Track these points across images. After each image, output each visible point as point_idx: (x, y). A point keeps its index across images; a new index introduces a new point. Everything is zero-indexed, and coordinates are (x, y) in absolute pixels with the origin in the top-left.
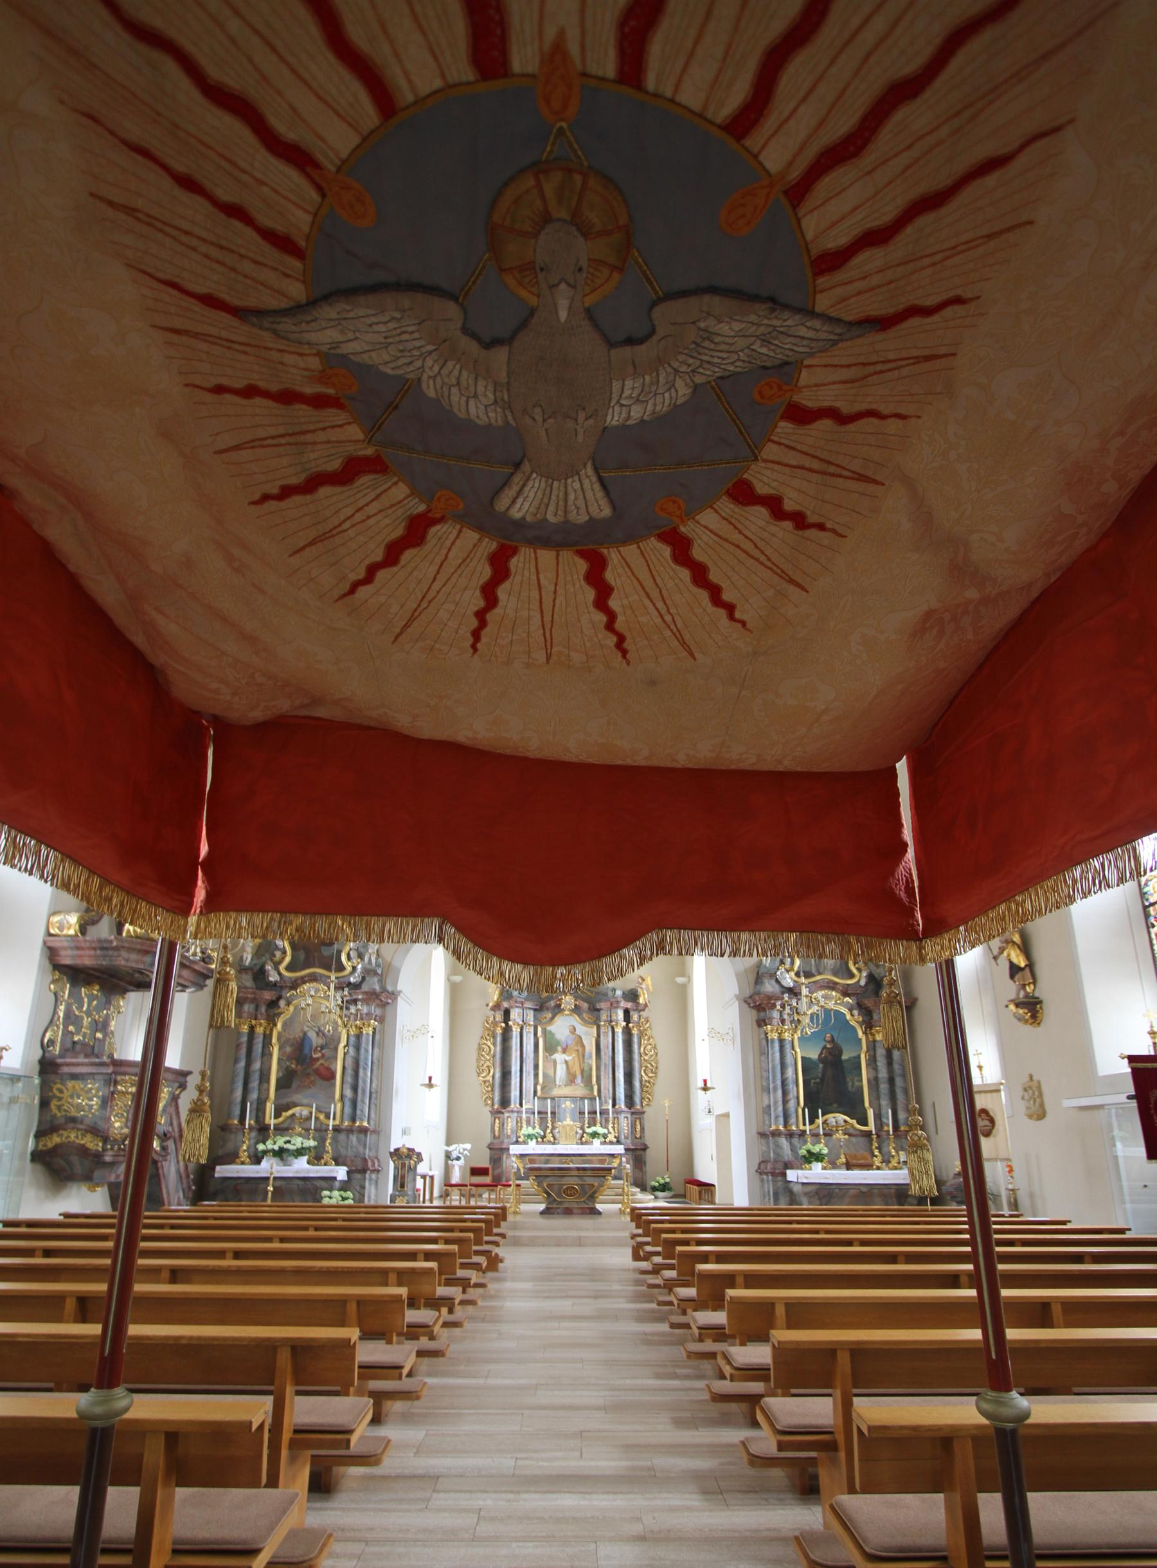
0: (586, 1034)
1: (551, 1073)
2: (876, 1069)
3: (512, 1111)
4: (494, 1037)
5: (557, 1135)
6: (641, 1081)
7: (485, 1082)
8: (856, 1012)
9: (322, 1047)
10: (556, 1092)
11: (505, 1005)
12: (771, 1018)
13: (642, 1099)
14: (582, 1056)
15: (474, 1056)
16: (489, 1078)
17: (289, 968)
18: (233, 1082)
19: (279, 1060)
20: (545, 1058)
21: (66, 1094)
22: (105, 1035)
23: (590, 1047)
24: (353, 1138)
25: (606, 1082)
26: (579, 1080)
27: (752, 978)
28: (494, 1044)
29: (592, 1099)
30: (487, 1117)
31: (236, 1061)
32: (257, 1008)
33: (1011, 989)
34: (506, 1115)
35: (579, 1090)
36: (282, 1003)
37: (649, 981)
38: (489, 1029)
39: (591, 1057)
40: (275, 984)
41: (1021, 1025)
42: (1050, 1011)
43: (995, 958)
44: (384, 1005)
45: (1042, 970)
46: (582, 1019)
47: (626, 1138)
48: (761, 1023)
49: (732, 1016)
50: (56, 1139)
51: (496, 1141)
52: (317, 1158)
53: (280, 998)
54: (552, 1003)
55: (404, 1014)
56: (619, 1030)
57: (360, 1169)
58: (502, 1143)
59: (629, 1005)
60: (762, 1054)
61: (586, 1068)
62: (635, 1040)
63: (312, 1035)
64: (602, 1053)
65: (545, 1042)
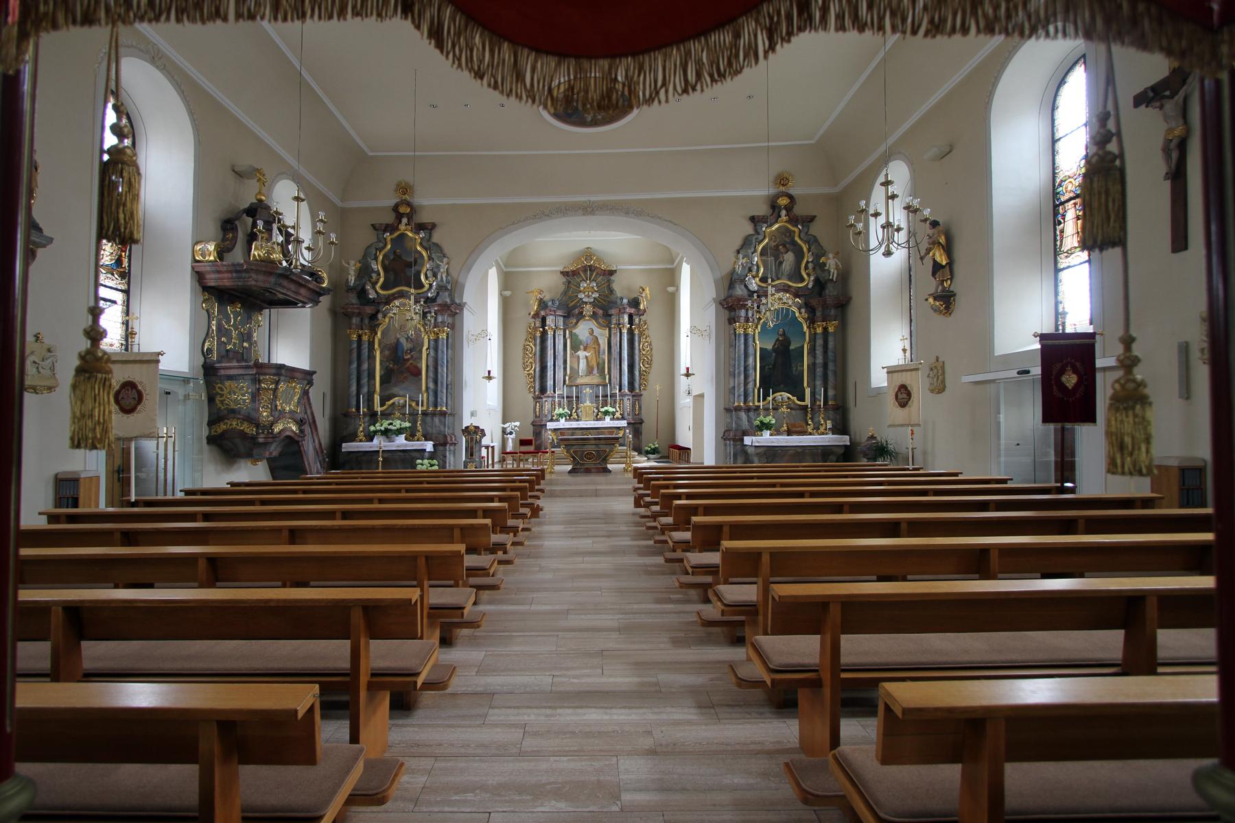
2: (815, 357)
8: (803, 310)
9: (411, 350)
10: (579, 381)
11: (543, 313)
12: (739, 317)
14: (598, 352)
15: (521, 355)
17: (383, 287)
18: (350, 380)
19: (381, 361)
20: (572, 354)
21: (225, 392)
22: (251, 345)
23: (603, 343)
24: (436, 420)
25: (615, 373)
26: (595, 371)
27: (727, 284)
29: (605, 386)
31: (350, 363)
32: (362, 320)
33: (931, 285)
35: (595, 379)
36: (380, 316)
37: (647, 291)
40: (374, 301)
41: (935, 315)
42: (961, 304)
43: (922, 258)
44: (454, 315)
45: (959, 268)
48: (732, 321)
49: (710, 315)
50: (223, 427)
52: (411, 436)
53: (378, 312)
54: (577, 311)
55: (469, 321)
56: (625, 331)
57: (442, 443)
59: (633, 311)
60: (731, 346)
63: (403, 341)
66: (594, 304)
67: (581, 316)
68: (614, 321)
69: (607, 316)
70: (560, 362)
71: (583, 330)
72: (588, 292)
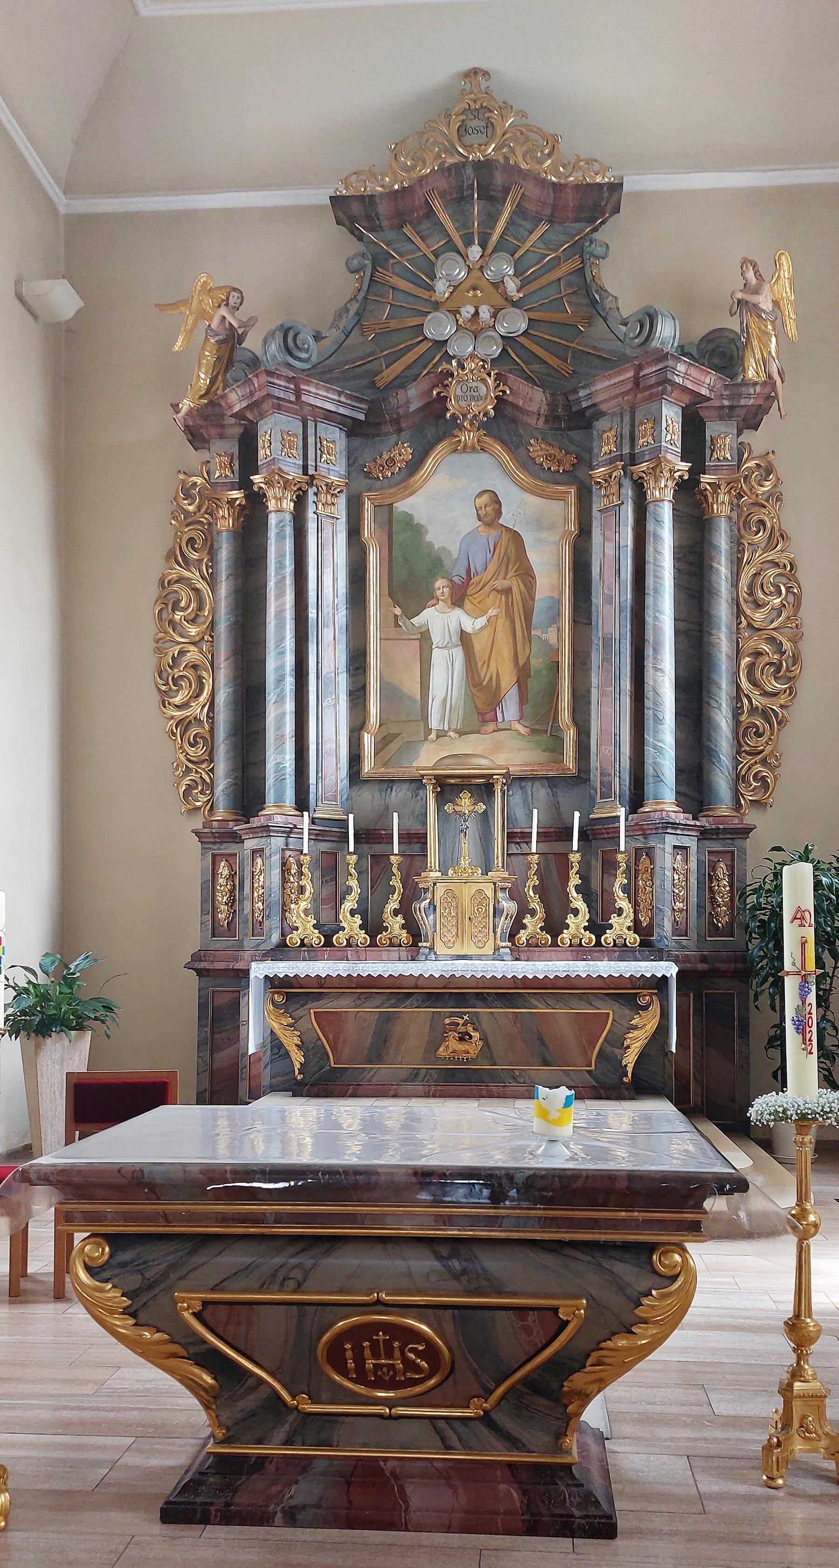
0: (540, 523)
1: (411, 685)
3: (266, 830)
4: (212, 552)
5: (426, 922)
6: (736, 712)
7: (184, 724)
10: (427, 759)
13: (738, 779)
14: (522, 613)
15: (149, 627)
16: (197, 709)
25: (610, 715)
26: (510, 709)
28: (212, 581)
30: (191, 858)
34: (250, 844)
38: (190, 520)
39: (556, 617)
46: (527, 464)
47: (680, 930)
51: (222, 943)
58: (240, 947)
61: (536, 663)
62: (722, 540)
64: (597, 599)
65: (389, 563)
66: (511, 358)
67: (435, 424)
68: (607, 448)
69: (573, 420)
70: (330, 655)
71: (449, 497)
72: (472, 309)
